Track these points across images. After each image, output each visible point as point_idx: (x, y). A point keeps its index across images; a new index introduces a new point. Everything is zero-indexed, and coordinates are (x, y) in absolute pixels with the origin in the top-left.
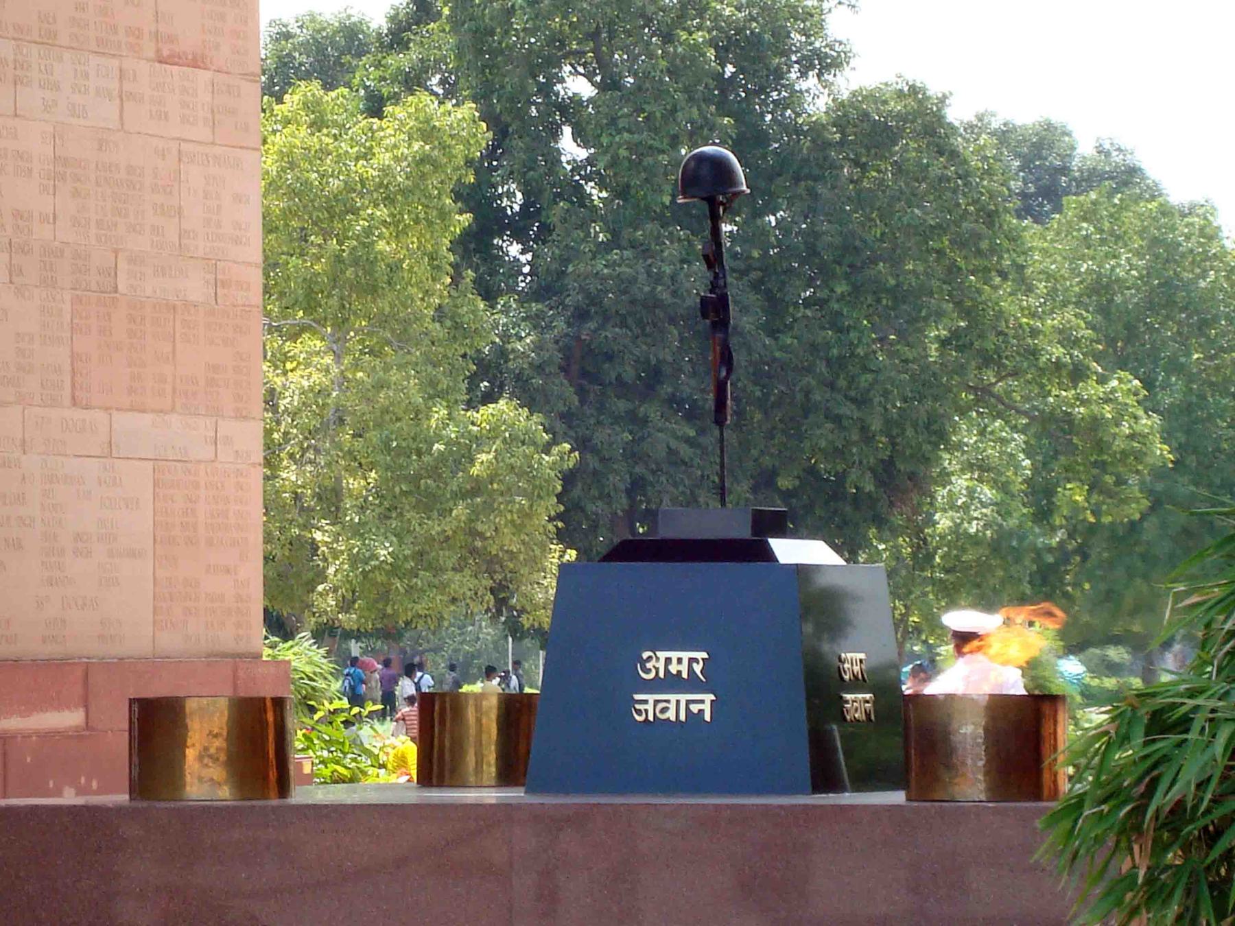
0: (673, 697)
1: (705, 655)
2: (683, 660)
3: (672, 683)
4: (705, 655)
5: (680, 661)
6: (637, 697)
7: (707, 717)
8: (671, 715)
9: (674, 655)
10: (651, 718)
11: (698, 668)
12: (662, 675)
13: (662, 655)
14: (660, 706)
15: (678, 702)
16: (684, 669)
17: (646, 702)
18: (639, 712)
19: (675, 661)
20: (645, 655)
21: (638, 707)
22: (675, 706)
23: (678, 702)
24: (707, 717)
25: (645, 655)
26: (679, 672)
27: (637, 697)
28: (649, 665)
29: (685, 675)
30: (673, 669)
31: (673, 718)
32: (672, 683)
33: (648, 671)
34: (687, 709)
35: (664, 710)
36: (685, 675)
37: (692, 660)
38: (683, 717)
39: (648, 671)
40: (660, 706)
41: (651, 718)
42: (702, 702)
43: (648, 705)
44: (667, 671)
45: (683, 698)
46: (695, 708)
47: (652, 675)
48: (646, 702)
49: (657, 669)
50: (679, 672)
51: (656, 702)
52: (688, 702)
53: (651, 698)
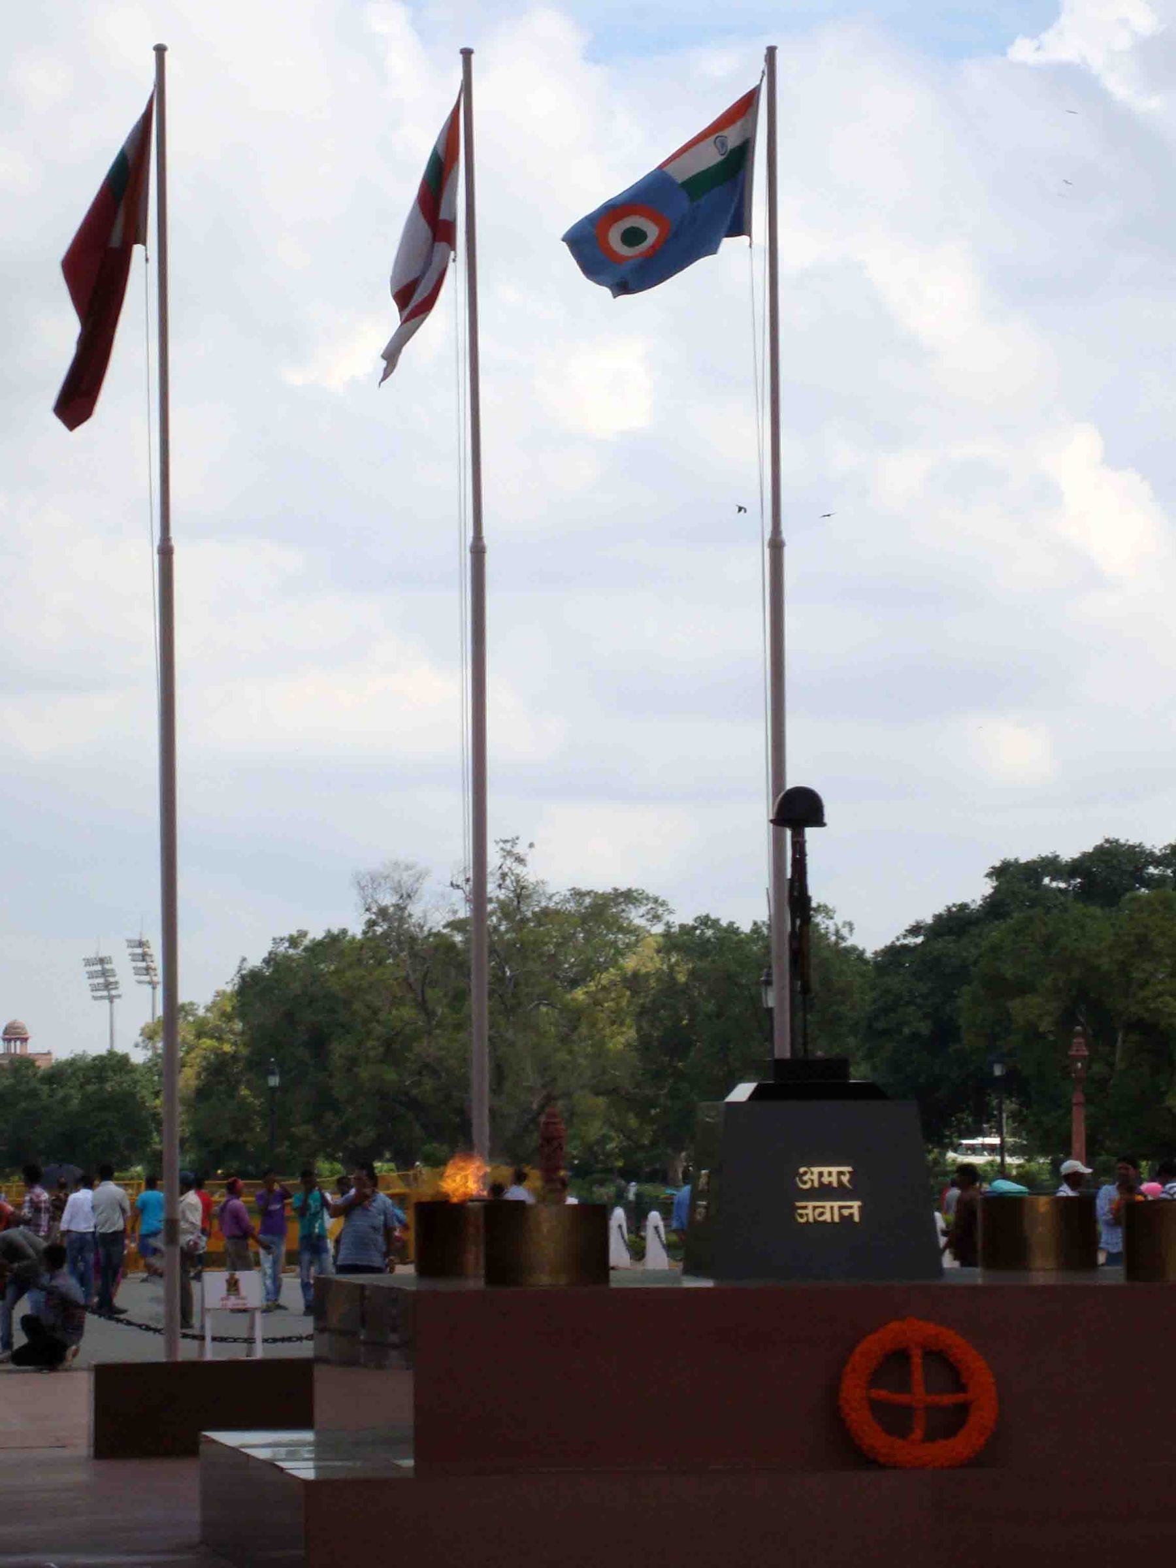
0: (828, 1204)
1: (849, 1169)
2: (833, 1174)
3: (824, 1192)
4: (849, 1169)
5: (830, 1174)
6: (799, 1204)
7: (856, 1219)
8: (827, 1217)
9: (825, 1170)
10: (811, 1220)
11: (845, 1179)
12: (816, 1184)
13: (816, 1170)
14: (818, 1211)
15: (832, 1208)
16: (834, 1180)
17: (805, 1208)
18: (801, 1216)
19: (826, 1174)
20: (802, 1170)
21: (800, 1211)
22: (830, 1211)
23: (832, 1208)
24: (856, 1219)
25: (802, 1170)
26: (830, 1183)
27: (799, 1204)
28: (805, 1178)
29: (835, 1184)
30: (826, 1180)
31: (829, 1220)
32: (824, 1192)
33: (805, 1183)
34: (841, 1215)
35: (821, 1214)
36: (835, 1184)
37: (840, 1173)
38: (837, 1219)
39: (805, 1183)
40: (818, 1211)
41: (811, 1220)
42: (851, 1207)
43: (809, 1211)
44: (821, 1183)
45: (836, 1204)
46: (846, 1212)
47: (808, 1186)
48: (805, 1208)
49: (812, 1181)
50: (830, 1183)
51: (815, 1208)
52: (841, 1208)
53: (811, 1204)
